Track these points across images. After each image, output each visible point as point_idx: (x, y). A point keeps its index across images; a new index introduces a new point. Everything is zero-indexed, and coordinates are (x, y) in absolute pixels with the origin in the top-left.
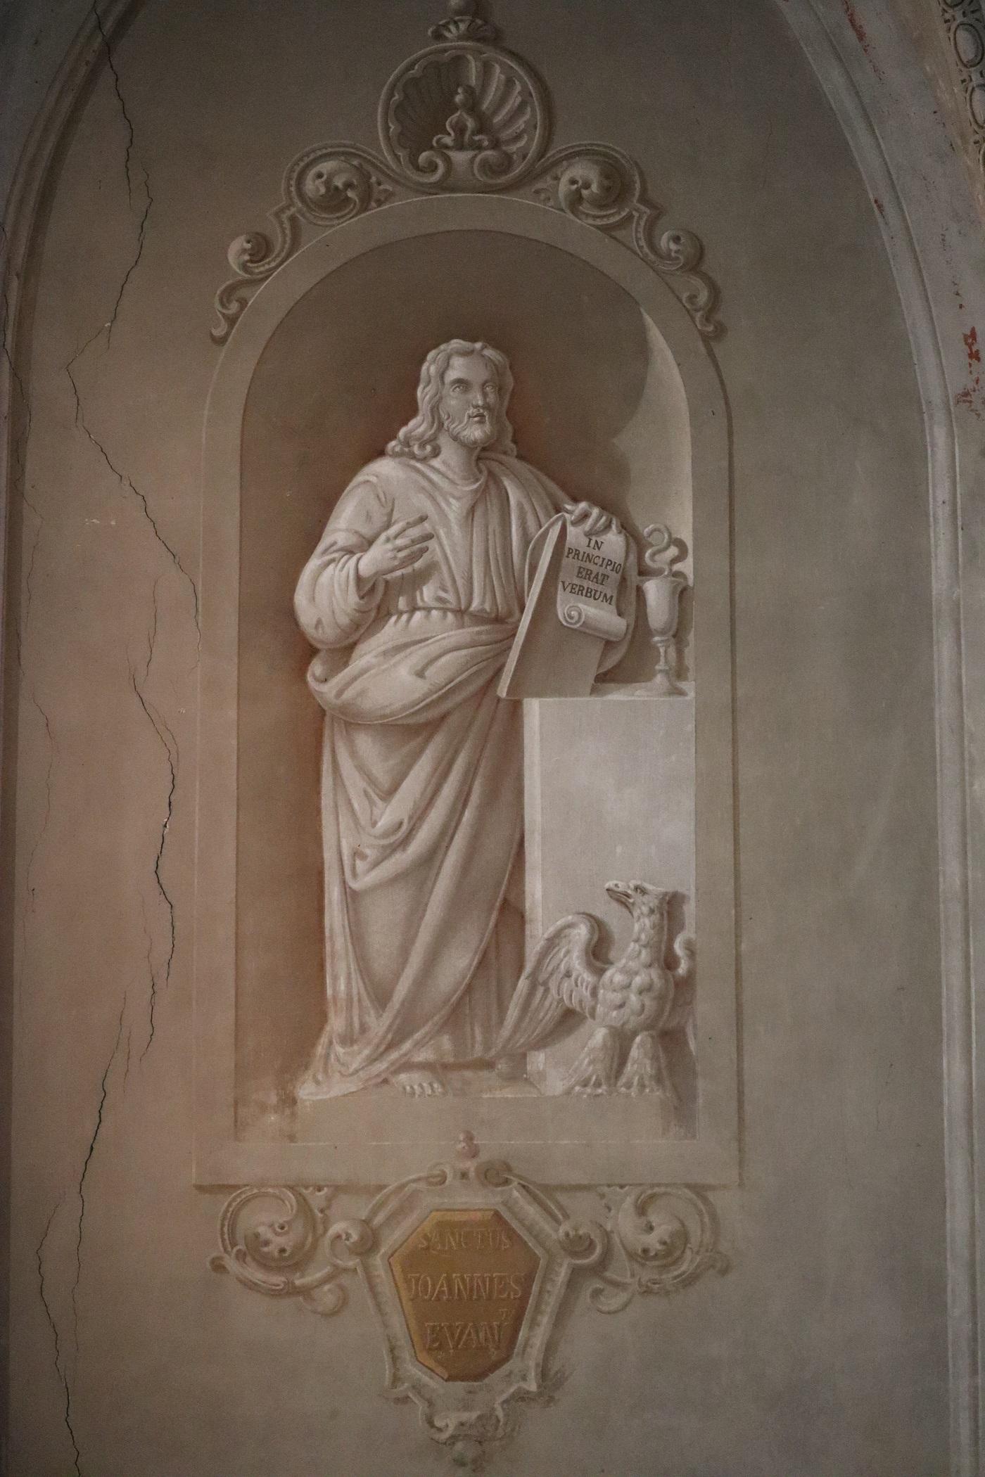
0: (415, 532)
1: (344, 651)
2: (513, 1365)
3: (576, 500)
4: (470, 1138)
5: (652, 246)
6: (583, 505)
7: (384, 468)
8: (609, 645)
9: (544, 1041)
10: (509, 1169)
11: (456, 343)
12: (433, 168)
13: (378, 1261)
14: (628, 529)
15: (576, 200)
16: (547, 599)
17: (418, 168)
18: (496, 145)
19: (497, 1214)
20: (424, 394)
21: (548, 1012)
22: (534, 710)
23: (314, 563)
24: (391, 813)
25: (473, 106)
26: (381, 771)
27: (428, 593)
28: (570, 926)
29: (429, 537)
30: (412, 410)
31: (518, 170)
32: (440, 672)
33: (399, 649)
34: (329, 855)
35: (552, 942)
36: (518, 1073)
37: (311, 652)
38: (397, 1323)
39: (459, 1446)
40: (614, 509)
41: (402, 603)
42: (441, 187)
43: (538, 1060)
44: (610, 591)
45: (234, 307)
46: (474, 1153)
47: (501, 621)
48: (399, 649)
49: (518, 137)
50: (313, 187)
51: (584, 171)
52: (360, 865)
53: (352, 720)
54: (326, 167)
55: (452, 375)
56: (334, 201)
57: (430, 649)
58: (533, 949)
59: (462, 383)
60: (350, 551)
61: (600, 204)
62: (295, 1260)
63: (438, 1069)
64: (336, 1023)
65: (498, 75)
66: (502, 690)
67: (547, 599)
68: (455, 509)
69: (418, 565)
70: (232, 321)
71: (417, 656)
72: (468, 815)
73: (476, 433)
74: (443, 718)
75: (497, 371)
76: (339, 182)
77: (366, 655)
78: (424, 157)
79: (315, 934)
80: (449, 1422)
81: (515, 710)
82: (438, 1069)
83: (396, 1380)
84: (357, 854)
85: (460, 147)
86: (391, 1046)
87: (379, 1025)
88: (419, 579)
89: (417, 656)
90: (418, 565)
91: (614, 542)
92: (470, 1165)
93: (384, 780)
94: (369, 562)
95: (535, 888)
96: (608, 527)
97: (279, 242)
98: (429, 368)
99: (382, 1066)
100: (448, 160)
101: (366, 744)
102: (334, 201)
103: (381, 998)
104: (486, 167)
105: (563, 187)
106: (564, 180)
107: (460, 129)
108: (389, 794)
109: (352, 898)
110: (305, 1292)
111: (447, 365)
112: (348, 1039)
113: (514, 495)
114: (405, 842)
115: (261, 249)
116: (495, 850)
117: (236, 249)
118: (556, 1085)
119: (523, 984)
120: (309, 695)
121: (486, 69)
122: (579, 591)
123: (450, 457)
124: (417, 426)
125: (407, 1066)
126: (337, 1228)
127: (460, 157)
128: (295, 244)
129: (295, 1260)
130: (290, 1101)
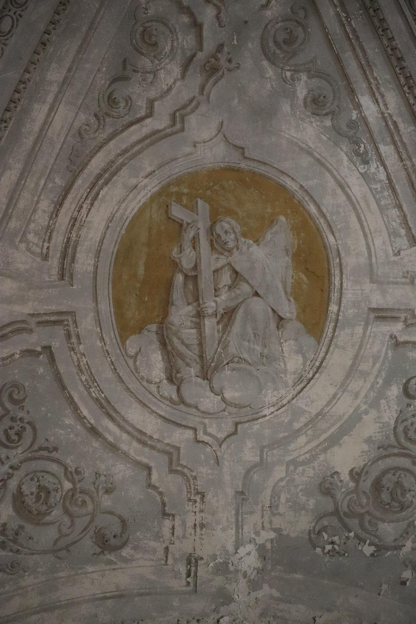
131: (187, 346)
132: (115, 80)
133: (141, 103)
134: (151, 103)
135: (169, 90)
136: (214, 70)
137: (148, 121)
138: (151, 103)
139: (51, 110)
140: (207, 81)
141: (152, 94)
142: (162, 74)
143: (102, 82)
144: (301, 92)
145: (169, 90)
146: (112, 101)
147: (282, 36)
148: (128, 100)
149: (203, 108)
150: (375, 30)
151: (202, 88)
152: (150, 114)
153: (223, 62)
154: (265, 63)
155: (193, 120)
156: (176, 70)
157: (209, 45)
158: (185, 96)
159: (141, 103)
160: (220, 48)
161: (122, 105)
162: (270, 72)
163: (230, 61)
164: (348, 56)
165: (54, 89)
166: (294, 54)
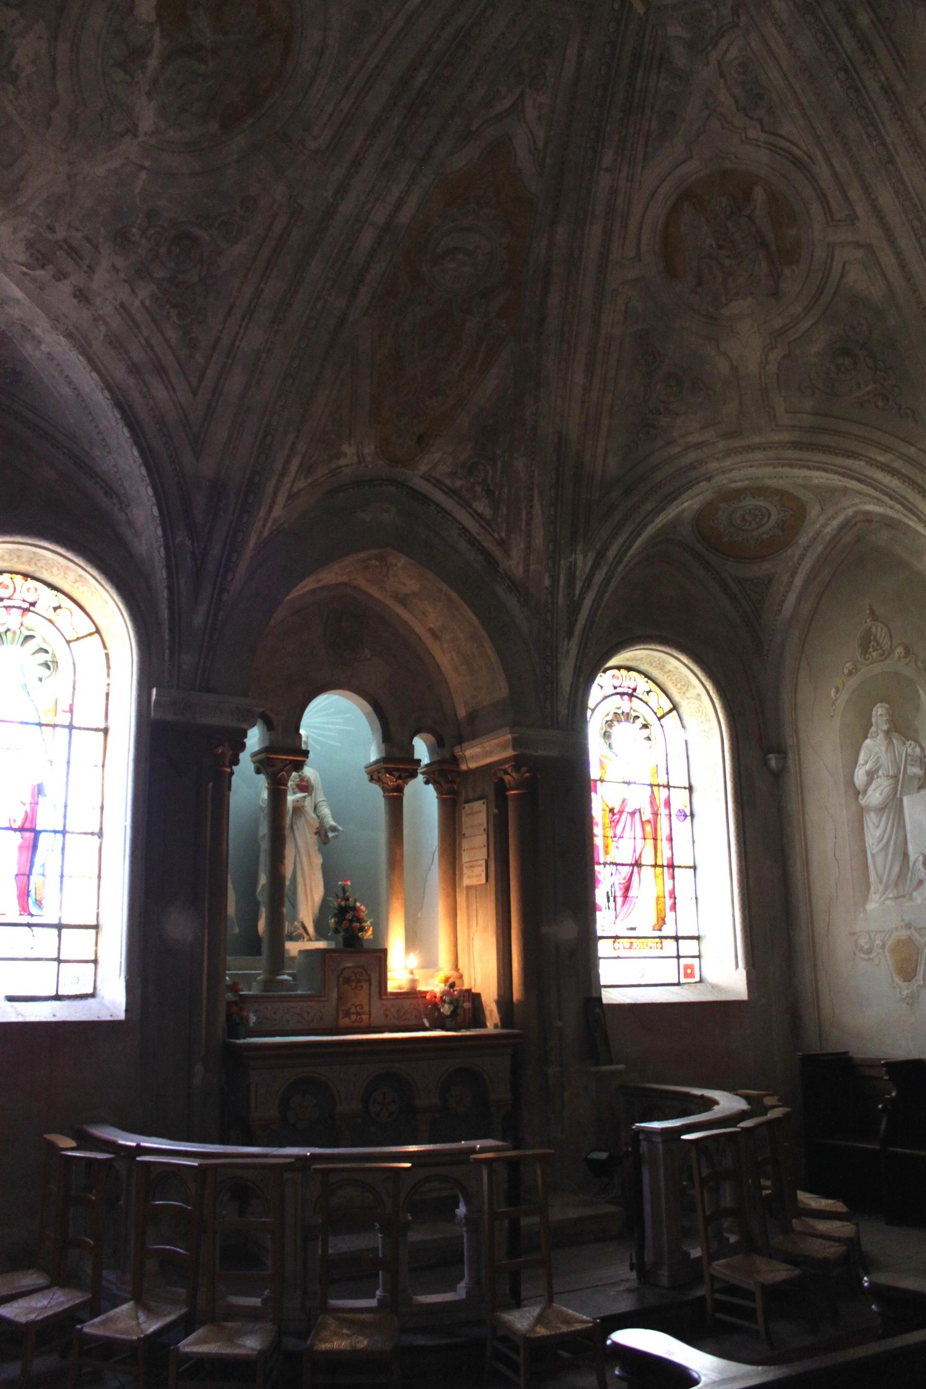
0: (876, 757)
1: (865, 791)
2: (917, 977)
3: (908, 740)
4: (902, 917)
5: (916, 665)
6: (910, 742)
7: (868, 741)
8: (920, 779)
9: (915, 890)
10: (911, 924)
11: (879, 705)
12: (869, 658)
13: (886, 951)
14: (921, 747)
15: (899, 658)
16: (905, 769)
17: (866, 660)
18: (881, 648)
19: (910, 937)
20: (874, 720)
21: (915, 882)
22: (906, 800)
23: (857, 770)
24: (878, 833)
25: (875, 639)
26: (875, 820)
27: (880, 773)
28: (918, 857)
29: (879, 758)
30: (872, 725)
31: (886, 653)
32: (885, 793)
33: (876, 788)
34: (867, 845)
35: (915, 862)
36: (911, 898)
37: (859, 793)
38: (891, 968)
39: (908, 999)
40: (916, 741)
41: (875, 776)
42: (871, 663)
43: (915, 894)
44: (918, 763)
45: (834, 707)
46: (903, 920)
47: (896, 777)
48: (876, 788)
49: (885, 645)
50: (846, 671)
51: (900, 650)
52: (874, 847)
53: (868, 809)
54: (848, 665)
55: (879, 713)
56: (850, 674)
57: (882, 787)
58: (911, 864)
59: (881, 715)
60: (864, 765)
61: (905, 657)
62: (869, 951)
63: (895, 898)
64: (872, 889)
65: (879, 630)
66: (898, 796)
67: (905, 769)
68: (883, 749)
69: (878, 765)
70: (834, 710)
71: (879, 790)
72: (895, 830)
73: (885, 727)
74: (887, 804)
75: (887, 709)
76: (850, 668)
77: (870, 792)
78: (867, 656)
79: (867, 867)
80: (905, 993)
81: (901, 800)
82: (895, 898)
83: (893, 982)
84: (873, 844)
85: (874, 651)
86: (884, 893)
87: (881, 888)
88: (877, 771)
89: (879, 790)
90: (878, 765)
91: (918, 749)
92: (903, 924)
93: (876, 824)
94: (867, 767)
95: (911, 848)
96: (916, 747)
97: (841, 688)
98: (874, 713)
99: (882, 899)
100: (872, 656)
101: (872, 815)
102: (850, 674)
103: (881, 882)
104: (881, 655)
105: (896, 655)
106: (896, 653)
107: (873, 646)
108: (878, 827)
109: (873, 855)
110: (872, 960)
111: (877, 711)
112: (875, 893)
113: (895, 742)
114: (882, 839)
115: (837, 691)
116: (901, 839)
117: (833, 691)
118: (919, 901)
119: (910, 874)
120: (859, 805)
121: (877, 629)
122: (912, 765)
123: (881, 736)
124: (873, 729)
125: (887, 899)
126: (877, 942)
127: (874, 654)
128: (844, 686)
129: (869, 951)
130: (865, 910)
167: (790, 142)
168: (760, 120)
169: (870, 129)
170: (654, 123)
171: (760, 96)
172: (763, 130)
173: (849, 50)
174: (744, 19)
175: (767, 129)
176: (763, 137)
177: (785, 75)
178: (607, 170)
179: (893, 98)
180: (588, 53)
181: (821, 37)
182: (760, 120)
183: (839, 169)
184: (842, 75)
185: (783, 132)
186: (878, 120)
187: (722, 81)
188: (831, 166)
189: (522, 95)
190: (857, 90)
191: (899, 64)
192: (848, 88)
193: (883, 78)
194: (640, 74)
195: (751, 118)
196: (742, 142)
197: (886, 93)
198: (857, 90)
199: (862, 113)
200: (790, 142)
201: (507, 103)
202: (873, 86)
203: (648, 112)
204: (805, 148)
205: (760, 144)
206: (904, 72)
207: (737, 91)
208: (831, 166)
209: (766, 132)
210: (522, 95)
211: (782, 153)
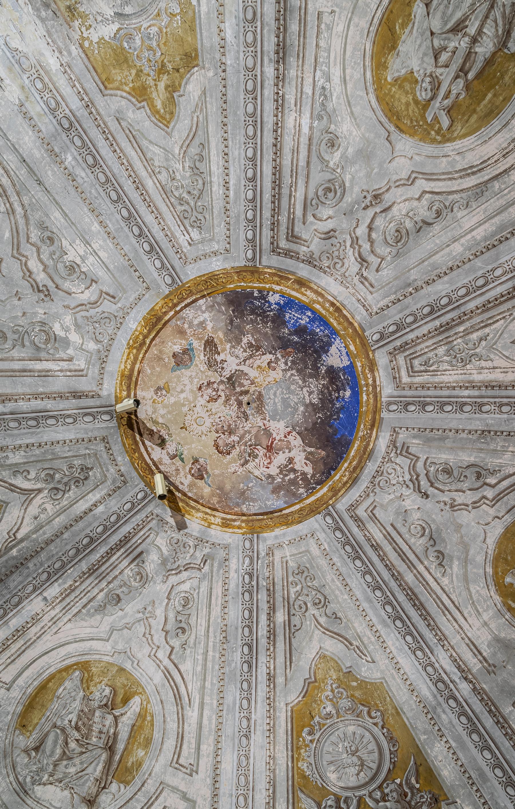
131: (495, 21)
132: (429, 224)
133: (424, 202)
134: (419, 199)
135: (405, 200)
136: (376, 197)
137: (427, 189)
138: (419, 199)
139: (473, 230)
140: (383, 193)
141: (415, 203)
142: (404, 212)
143: (437, 227)
144: (337, 155)
145: (405, 200)
146: (439, 213)
147: (331, 195)
148: (430, 209)
149: (395, 178)
150: (280, 172)
151: (388, 190)
152: (425, 192)
153: (369, 198)
154: (347, 185)
155: (404, 175)
156: (395, 209)
157: (370, 213)
158: (400, 190)
159: (424, 202)
160: (366, 208)
161: (435, 208)
162: (348, 178)
163: (365, 197)
164: (302, 163)
165: (463, 241)
166: (329, 181)
167: (183, 679)
168: (173, 648)
169: (245, 702)
170: (102, 594)
171: (184, 630)
172: (169, 657)
173: (260, 634)
174: (207, 567)
175: (173, 657)
176: (166, 662)
177: (209, 627)
178: (45, 599)
179: (272, 686)
180: (101, 508)
181: (246, 612)
182: (173, 648)
183: (205, 722)
184: (246, 649)
185: (182, 668)
186: (253, 699)
187: (166, 600)
188: (201, 715)
189: (40, 491)
190: (250, 667)
191: (288, 663)
192: (245, 662)
193: (272, 667)
194: (119, 554)
195: (167, 643)
196: (149, 656)
197: (269, 680)
198: (250, 667)
199: (245, 685)
200: (183, 679)
201: (26, 485)
202: (262, 671)
203: (104, 584)
204: (190, 691)
205: (162, 667)
206: (288, 670)
207: (171, 615)
208: (201, 715)
209: (170, 660)
210: (40, 491)
211: (172, 684)
